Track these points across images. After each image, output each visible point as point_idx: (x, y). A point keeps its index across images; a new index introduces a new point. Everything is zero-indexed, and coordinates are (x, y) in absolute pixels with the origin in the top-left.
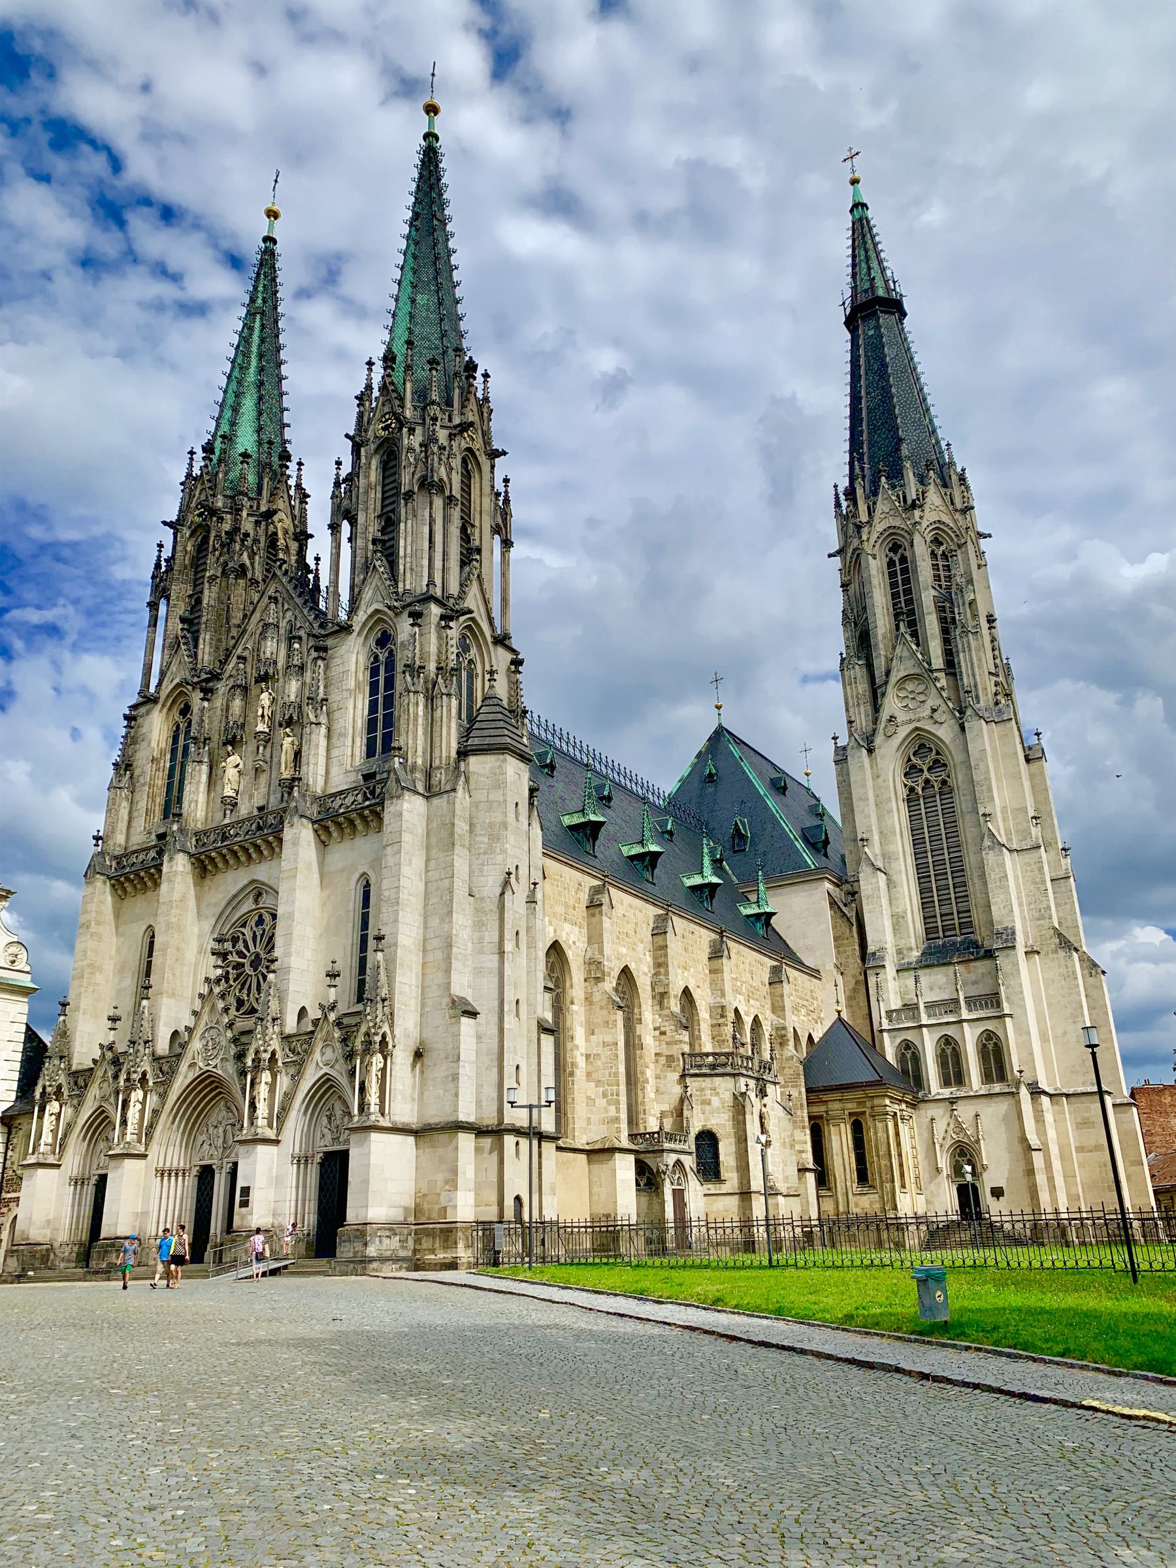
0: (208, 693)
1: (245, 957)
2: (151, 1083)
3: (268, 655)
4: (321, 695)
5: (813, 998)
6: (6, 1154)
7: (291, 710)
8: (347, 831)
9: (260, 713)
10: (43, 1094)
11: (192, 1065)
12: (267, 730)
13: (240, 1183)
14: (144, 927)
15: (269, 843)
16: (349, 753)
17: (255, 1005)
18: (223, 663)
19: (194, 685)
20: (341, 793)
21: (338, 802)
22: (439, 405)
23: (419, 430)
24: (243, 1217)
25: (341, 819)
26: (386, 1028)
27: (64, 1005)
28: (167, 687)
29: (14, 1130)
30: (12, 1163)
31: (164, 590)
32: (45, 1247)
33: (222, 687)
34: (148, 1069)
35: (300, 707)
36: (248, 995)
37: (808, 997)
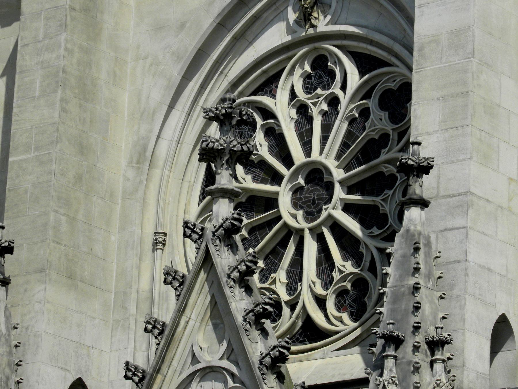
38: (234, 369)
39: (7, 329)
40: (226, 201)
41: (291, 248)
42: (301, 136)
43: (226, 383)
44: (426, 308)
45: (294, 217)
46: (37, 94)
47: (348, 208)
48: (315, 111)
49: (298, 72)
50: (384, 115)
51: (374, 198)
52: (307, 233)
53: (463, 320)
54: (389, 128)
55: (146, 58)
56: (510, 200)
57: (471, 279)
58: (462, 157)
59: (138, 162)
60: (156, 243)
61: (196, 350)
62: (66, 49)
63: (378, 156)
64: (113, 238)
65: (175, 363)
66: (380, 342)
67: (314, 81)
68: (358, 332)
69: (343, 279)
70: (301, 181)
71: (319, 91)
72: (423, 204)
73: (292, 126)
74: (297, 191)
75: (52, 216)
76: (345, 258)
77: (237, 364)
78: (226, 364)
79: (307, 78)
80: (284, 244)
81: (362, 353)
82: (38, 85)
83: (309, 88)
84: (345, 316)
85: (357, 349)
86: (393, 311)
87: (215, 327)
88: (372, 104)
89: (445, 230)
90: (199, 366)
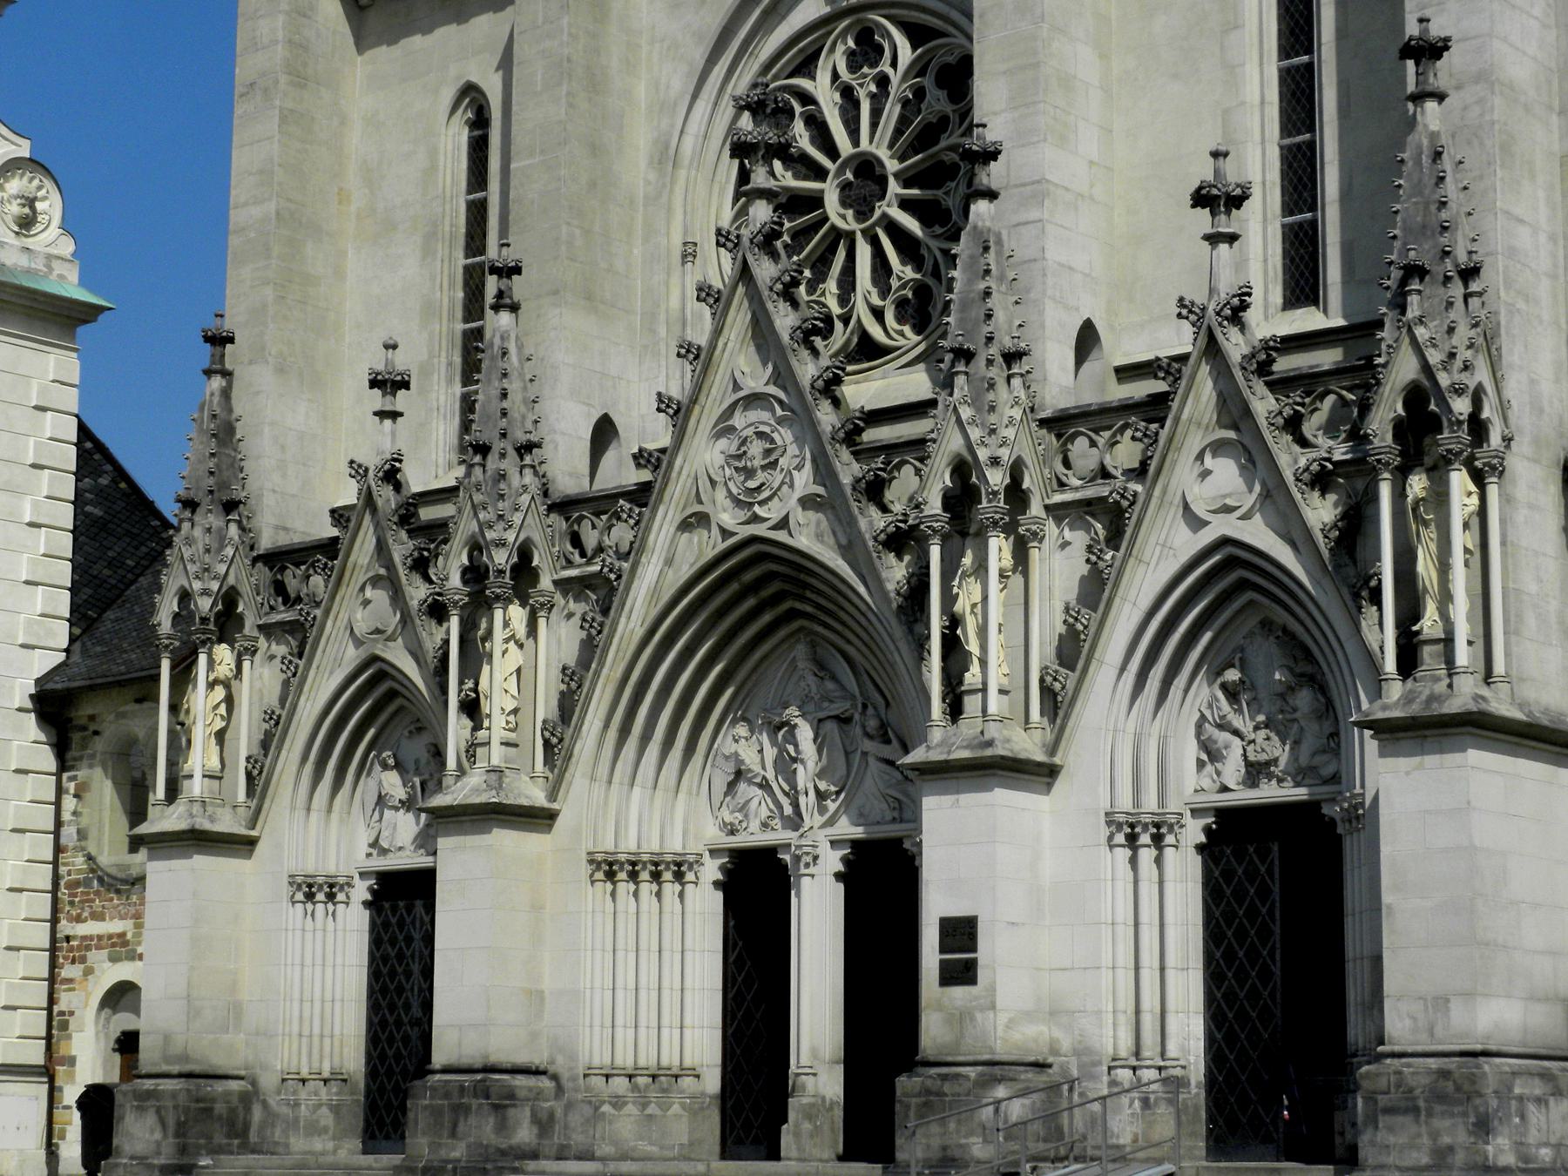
1: (820, 173)
2: (546, 582)
6: (58, 804)
10: (182, 618)
11: (696, 521)
13: (936, 905)
14: (448, 94)
17: (876, 332)
24: (961, 1019)
26: (1482, 375)
27: (219, 340)
29: (76, 737)
30: (82, 834)
32: (234, 1085)
34: (537, 537)
36: (844, 299)
38: (782, 395)
39: (520, 361)
40: (764, 202)
41: (841, 254)
42: (846, 123)
43: (773, 411)
44: (1000, 316)
45: (844, 217)
46: (539, 88)
47: (905, 204)
48: (862, 94)
49: (840, 48)
50: (942, 94)
51: (935, 192)
52: (859, 236)
53: (1043, 326)
54: (948, 108)
55: (663, 40)
56: (1092, 186)
57: (1050, 281)
58: (1035, 139)
59: (660, 163)
60: (684, 256)
61: (738, 375)
62: (570, 34)
63: (937, 142)
64: (635, 251)
65: (714, 391)
66: (948, 357)
67: (859, 59)
68: (922, 347)
69: (903, 287)
70: (849, 175)
71: (865, 70)
72: (992, 195)
73: (836, 112)
74: (845, 187)
75: (564, 229)
76: (904, 263)
77: (784, 389)
78: (772, 390)
79: (851, 55)
80: (832, 249)
81: (928, 371)
82: (539, 77)
83: (853, 67)
84: (907, 329)
85: (922, 366)
86: (961, 321)
87: (759, 348)
88: (928, 82)
89: (1018, 225)
90: (741, 394)
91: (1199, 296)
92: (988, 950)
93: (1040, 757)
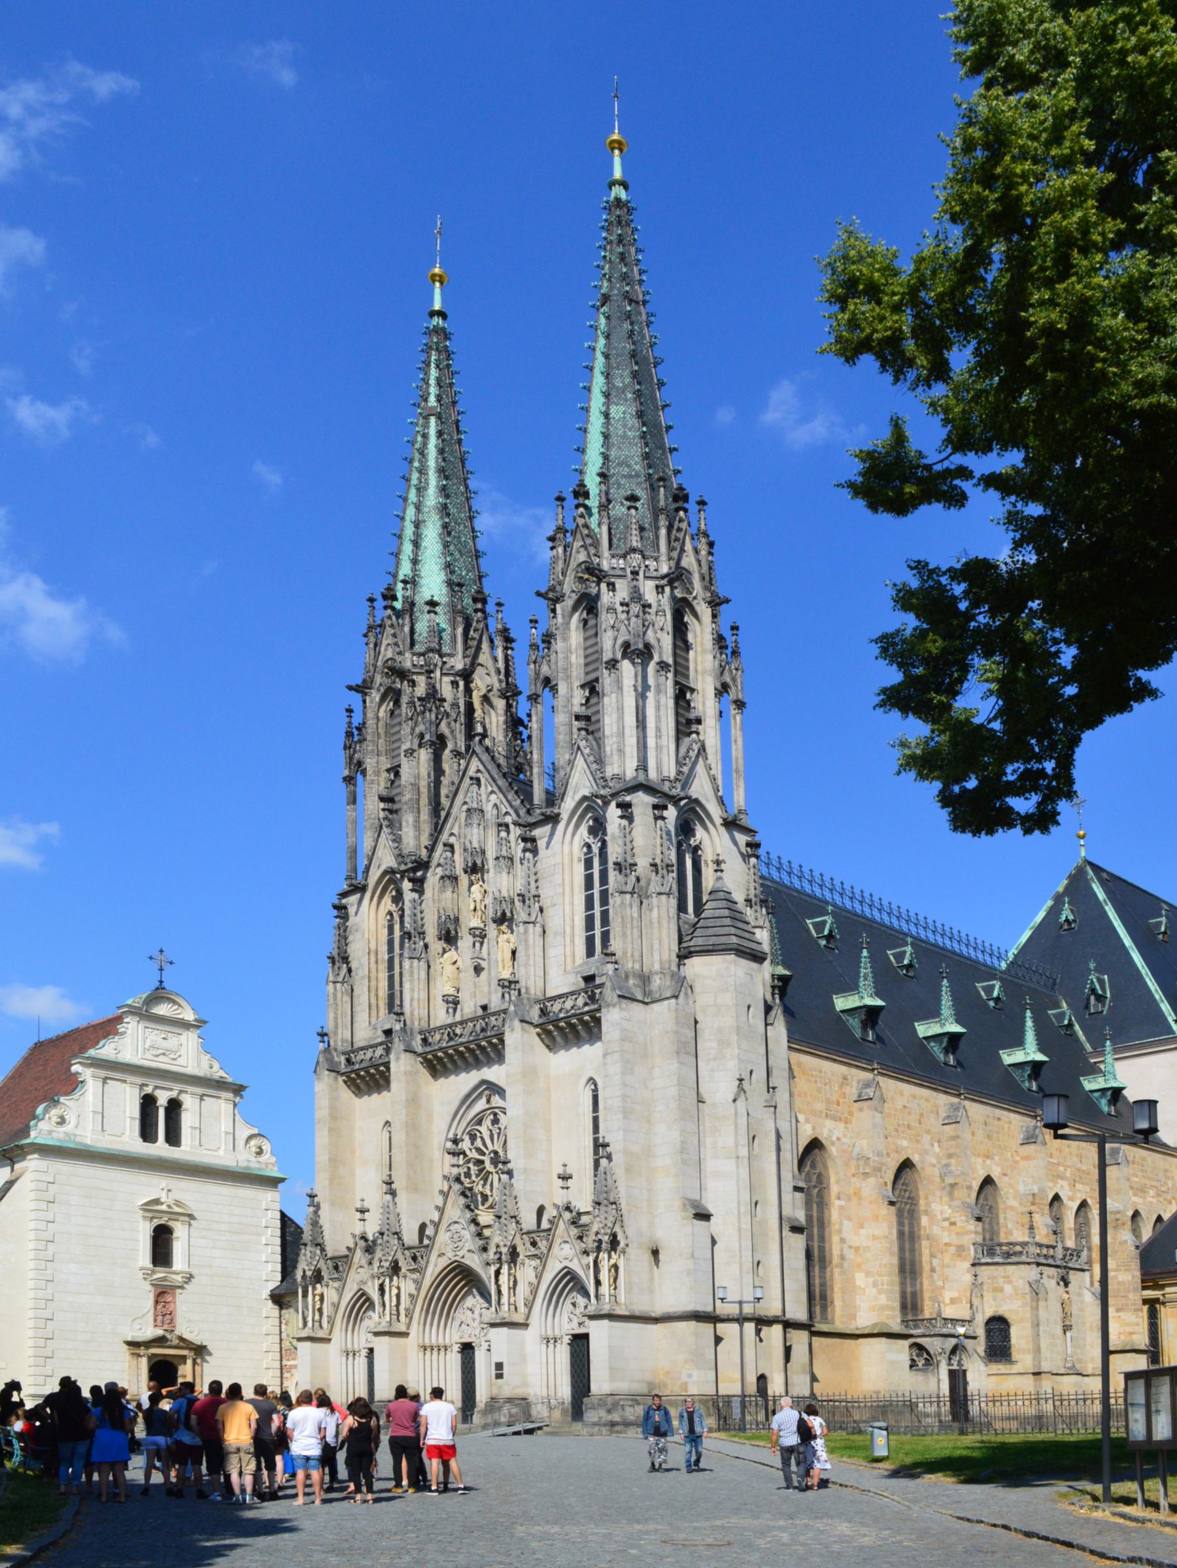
0: (419, 885)
3: (475, 844)
4: (533, 892)
5: (1167, 1178)
7: (504, 905)
8: (570, 1036)
9: (472, 907)
12: (482, 926)
15: (494, 1046)
16: (568, 953)
18: (431, 849)
19: (403, 873)
20: (560, 996)
21: (556, 1007)
22: (641, 552)
23: (620, 584)
25: (562, 1024)
28: (374, 875)
31: (359, 764)
33: (432, 879)
35: (513, 902)
37: (1161, 1176)
91: (559, 1203)
92: (505, 1371)
93: (521, 1321)
